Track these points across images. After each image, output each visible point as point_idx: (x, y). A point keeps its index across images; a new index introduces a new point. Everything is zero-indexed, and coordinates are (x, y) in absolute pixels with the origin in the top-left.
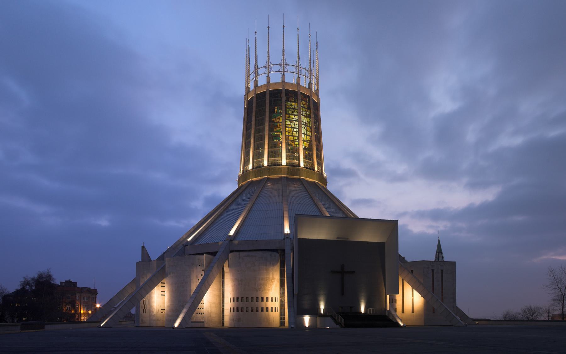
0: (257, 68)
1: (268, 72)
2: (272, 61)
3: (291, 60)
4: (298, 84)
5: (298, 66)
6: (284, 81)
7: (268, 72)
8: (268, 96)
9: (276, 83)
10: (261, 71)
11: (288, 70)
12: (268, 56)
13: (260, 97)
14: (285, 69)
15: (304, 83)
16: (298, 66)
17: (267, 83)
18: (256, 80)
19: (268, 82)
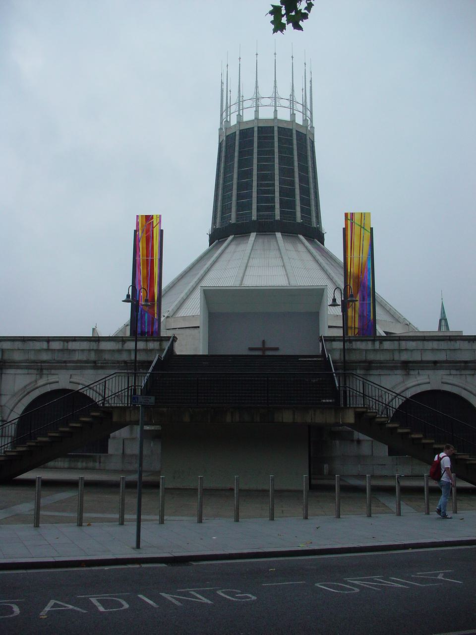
0: (240, 101)
1: (257, 106)
2: (261, 94)
3: (284, 92)
4: (293, 121)
5: (292, 101)
6: (276, 118)
7: (257, 106)
8: (256, 134)
10: (246, 104)
12: (257, 87)
13: (246, 134)
14: (277, 103)
15: (299, 120)
16: (292, 101)
17: (255, 118)
18: (239, 114)
19: (257, 118)
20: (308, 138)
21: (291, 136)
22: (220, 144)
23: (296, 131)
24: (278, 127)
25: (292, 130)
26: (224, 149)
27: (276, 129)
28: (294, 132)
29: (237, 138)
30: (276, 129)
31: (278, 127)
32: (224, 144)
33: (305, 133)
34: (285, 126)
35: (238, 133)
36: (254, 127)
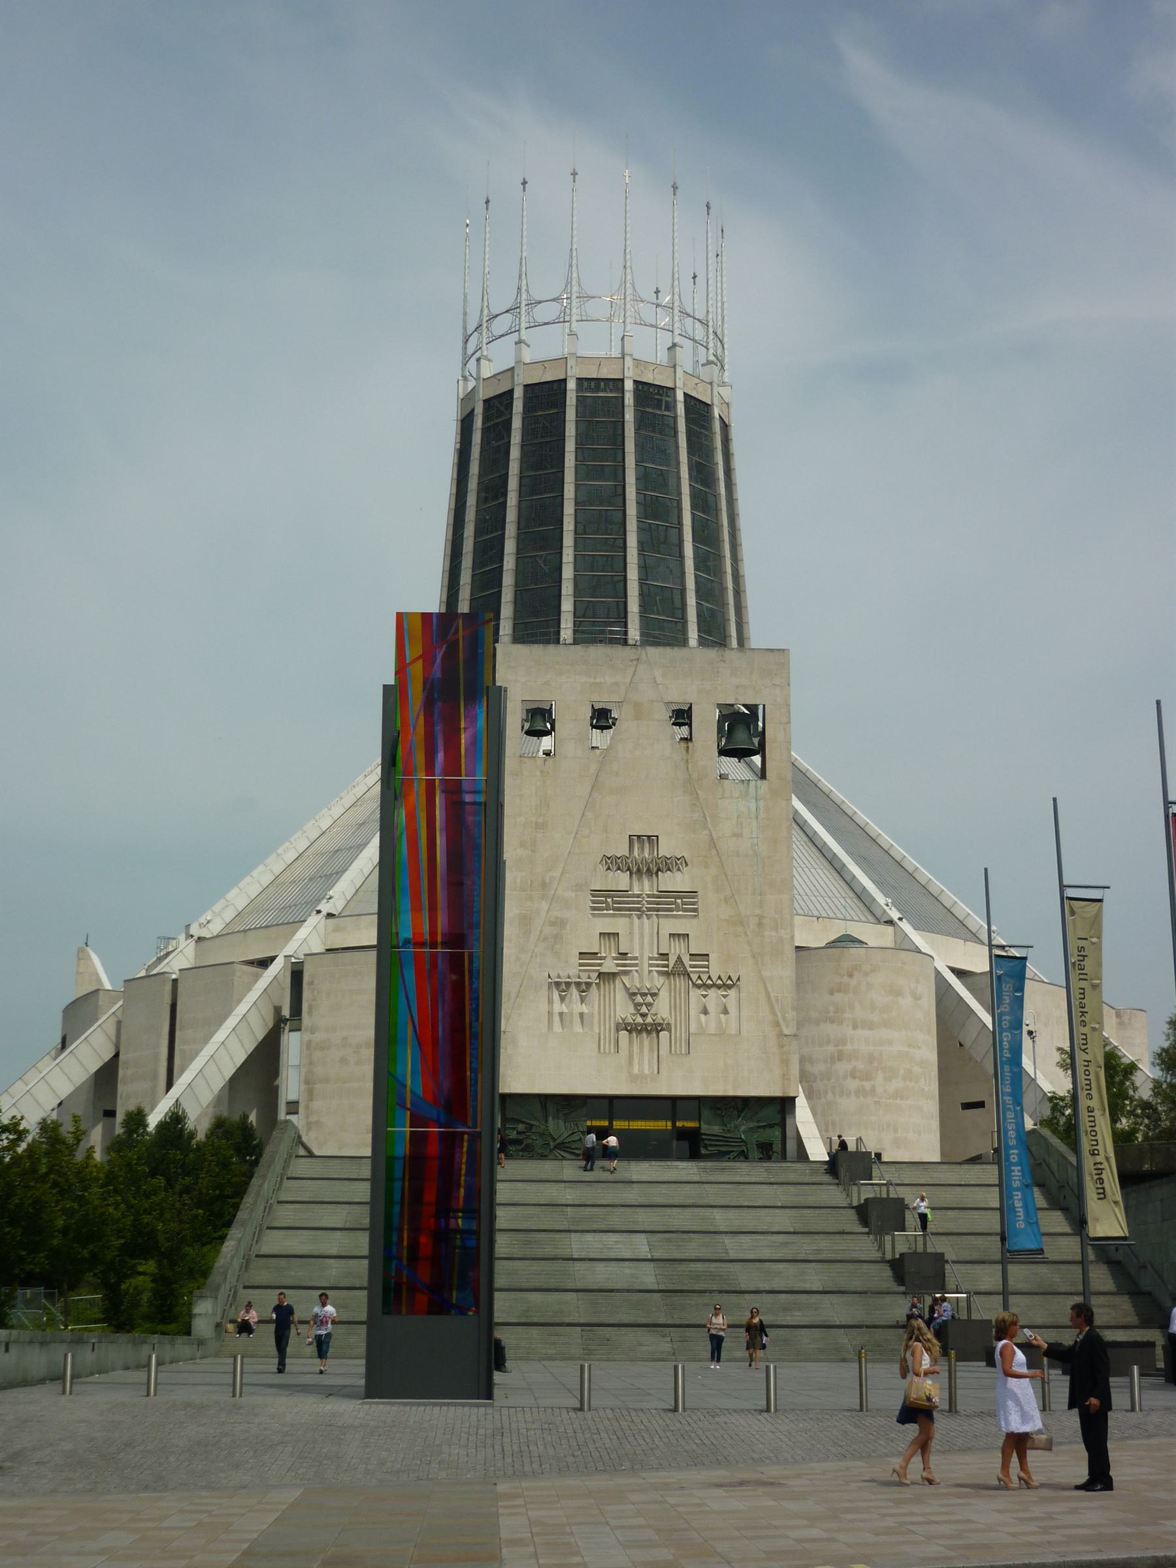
9: (600, 361)
11: (641, 319)
20: (717, 416)
21: (671, 406)
22: (466, 424)
23: (685, 393)
24: (635, 381)
25: (673, 389)
26: (477, 438)
27: (629, 385)
28: (680, 396)
29: (518, 406)
30: (629, 385)
31: (634, 381)
32: (478, 422)
33: (710, 403)
34: (648, 378)
35: (518, 394)
36: (565, 381)
